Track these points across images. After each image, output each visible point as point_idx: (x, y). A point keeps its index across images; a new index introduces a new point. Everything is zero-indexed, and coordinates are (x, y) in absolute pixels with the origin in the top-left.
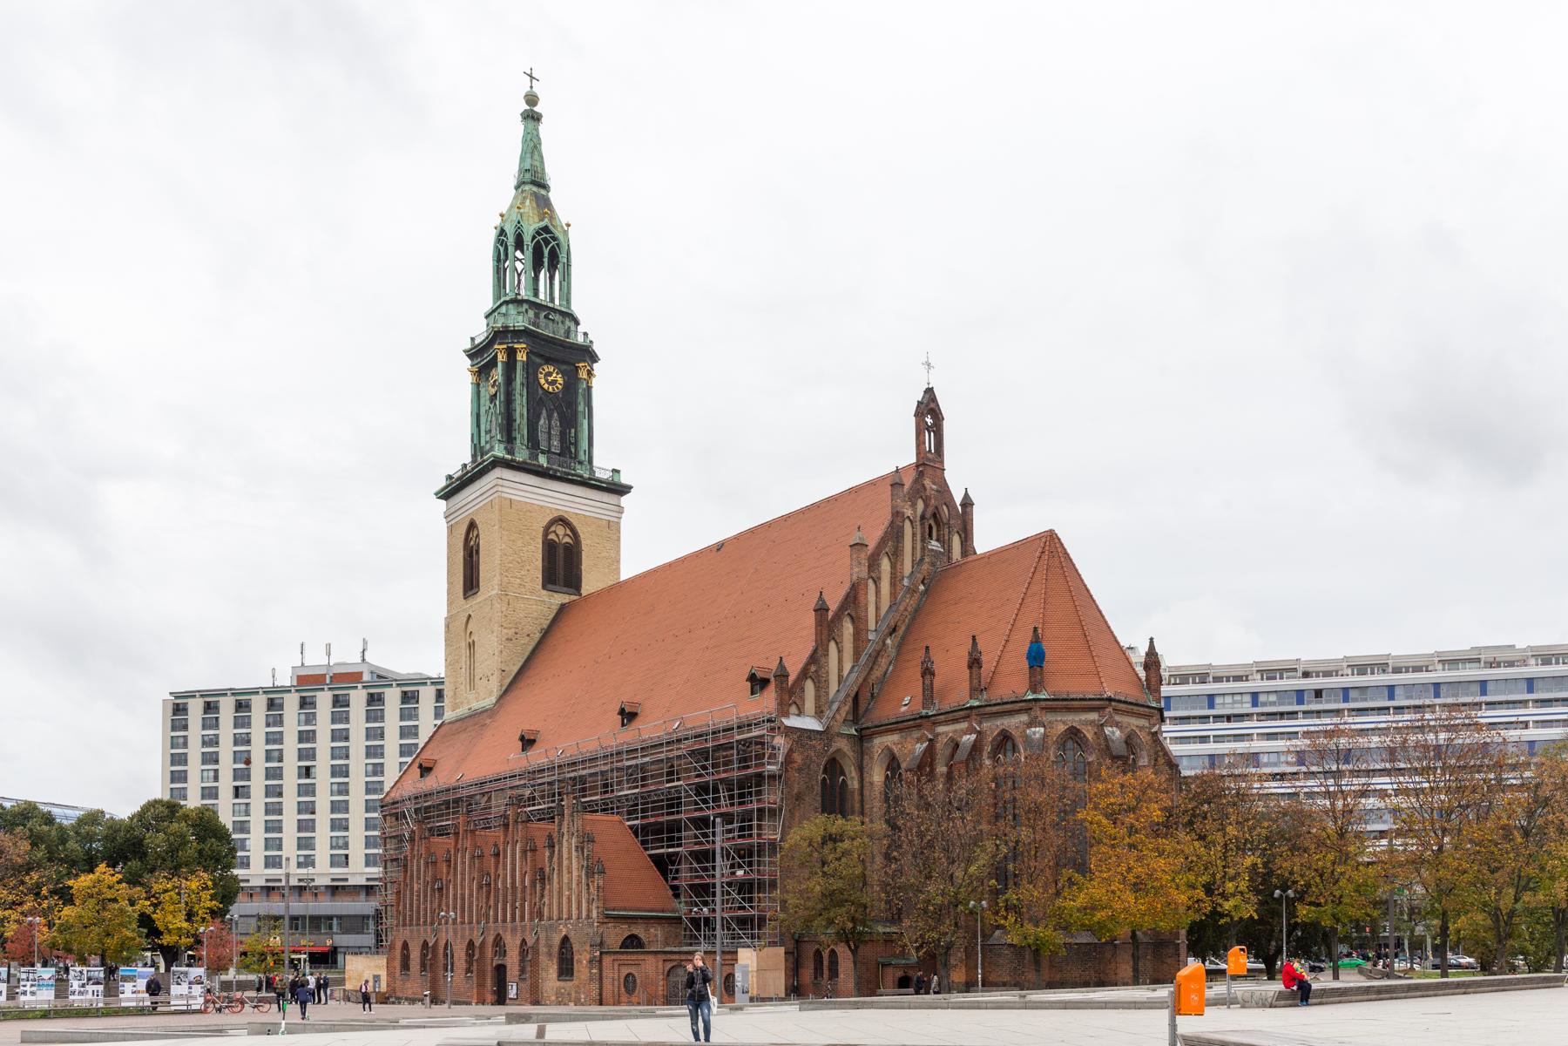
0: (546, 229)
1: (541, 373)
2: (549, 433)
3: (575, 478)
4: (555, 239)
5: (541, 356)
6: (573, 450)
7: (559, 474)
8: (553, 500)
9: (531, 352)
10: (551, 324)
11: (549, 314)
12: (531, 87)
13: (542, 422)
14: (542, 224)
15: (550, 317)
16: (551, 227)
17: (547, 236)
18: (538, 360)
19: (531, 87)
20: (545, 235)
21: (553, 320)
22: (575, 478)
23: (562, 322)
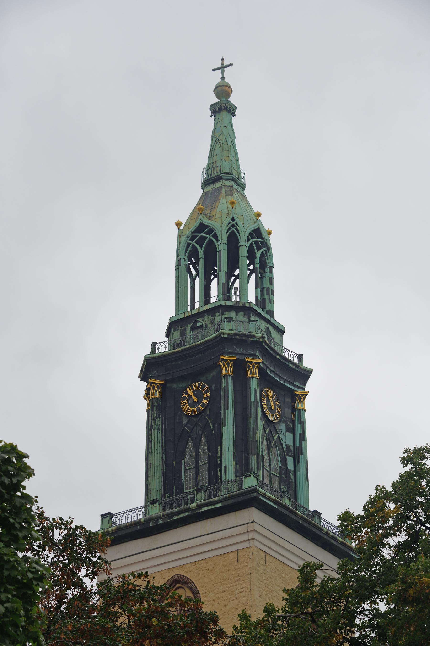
0: (202, 227)
1: (184, 398)
2: (197, 467)
3: (182, 515)
4: (211, 231)
5: (182, 379)
6: (219, 474)
7: (161, 522)
8: (163, 560)
9: (166, 382)
10: (200, 330)
11: (197, 322)
12: (223, 78)
13: (187, 457)
14: (197, 224)
15: (198, 325)
16: (206, 221)
18: (182, 385)
19: (223, 78)
20: (200, 235)
21: (201, 327)
22: (182, 515)
23: (212, 322)
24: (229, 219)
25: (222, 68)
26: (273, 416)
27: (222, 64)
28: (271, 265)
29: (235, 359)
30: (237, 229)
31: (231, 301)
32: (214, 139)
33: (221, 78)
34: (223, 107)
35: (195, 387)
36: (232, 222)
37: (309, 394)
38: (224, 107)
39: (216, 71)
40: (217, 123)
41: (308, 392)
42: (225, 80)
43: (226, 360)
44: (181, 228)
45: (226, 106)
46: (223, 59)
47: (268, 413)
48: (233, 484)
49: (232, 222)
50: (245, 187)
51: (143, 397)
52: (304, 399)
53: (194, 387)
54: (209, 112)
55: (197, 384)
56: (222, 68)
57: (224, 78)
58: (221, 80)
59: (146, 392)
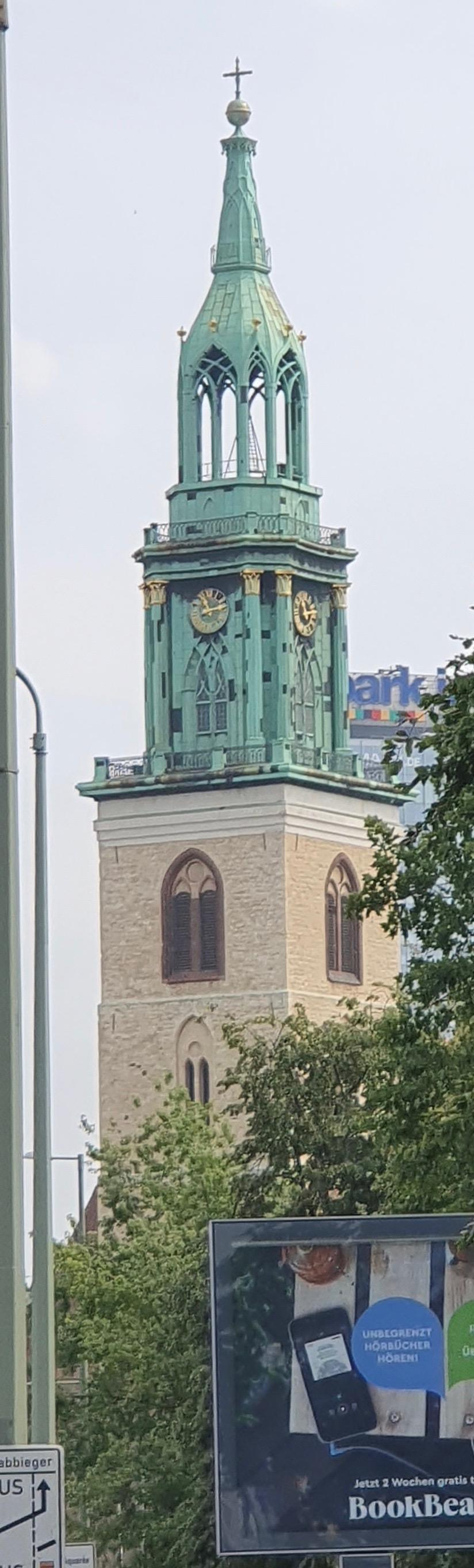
0: (215, 353)
4: (226, 362)
12: (238, 93)
19: (238, 93)
25: (237, 74)
30: (261, 362)
36: (257, 353)
44: (185, 338)
46: (237, 61)
47: (301, 627)
49: (257, 353)
52: (345, 592)
56: (237, 74)
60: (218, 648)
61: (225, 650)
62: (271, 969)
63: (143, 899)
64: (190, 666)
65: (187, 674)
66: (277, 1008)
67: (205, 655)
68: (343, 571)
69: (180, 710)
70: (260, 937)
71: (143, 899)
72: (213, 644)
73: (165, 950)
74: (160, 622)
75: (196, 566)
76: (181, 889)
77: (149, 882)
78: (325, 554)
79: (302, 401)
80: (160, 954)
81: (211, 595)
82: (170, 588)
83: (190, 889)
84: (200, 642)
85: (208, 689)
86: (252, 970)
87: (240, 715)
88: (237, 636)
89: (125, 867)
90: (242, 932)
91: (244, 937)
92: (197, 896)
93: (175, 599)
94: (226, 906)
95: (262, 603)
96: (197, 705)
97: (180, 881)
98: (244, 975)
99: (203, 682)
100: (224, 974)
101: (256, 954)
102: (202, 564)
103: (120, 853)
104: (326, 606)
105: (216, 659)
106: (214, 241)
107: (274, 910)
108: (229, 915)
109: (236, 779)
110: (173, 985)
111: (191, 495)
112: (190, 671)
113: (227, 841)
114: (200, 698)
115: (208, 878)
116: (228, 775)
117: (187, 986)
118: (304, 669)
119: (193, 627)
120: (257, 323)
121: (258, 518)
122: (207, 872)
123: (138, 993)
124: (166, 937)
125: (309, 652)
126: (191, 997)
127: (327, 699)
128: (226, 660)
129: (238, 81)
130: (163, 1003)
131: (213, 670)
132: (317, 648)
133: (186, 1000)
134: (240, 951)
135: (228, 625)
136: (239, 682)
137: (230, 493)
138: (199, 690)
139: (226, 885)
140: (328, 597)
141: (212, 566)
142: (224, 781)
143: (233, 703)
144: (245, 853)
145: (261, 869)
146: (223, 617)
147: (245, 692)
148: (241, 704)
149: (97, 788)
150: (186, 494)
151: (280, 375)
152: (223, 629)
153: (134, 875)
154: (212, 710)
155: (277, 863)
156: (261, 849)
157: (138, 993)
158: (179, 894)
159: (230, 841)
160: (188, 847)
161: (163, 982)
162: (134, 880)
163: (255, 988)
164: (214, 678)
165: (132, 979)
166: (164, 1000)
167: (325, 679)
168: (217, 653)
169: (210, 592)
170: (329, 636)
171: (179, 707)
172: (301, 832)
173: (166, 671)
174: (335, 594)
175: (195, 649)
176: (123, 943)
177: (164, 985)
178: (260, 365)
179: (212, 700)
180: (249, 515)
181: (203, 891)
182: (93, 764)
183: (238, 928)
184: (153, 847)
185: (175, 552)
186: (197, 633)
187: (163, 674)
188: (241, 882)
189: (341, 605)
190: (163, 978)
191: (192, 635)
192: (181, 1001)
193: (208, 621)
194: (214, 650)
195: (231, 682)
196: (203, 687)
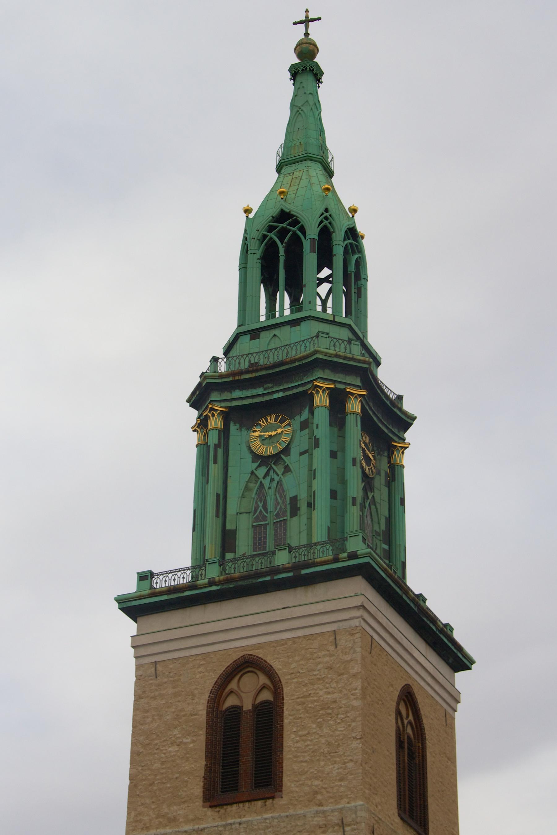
4: (296, 222)
12: (307, 34)
17: (284, 225)
19: (307, 34)
20: (281, 225)
24: (322, 210)
25: (307, 21)
26: (369, 469)
27: (307, 17)
28: (365, 277)
29: (332, 386)
30: (330, 223)
31: (326, 313)
32: (295, 110)
33: (305, 34)
34: (308, 69)
35: (270, 419)
36: (325, 214)
37: (410, 446)
38: (309, 68)
39: (297, 25)
40: (299, 88)
41: (409, 444)
42: (310, 37)
43: (320, 387)
44: (251, 216)
45: (311, 69)
46: (307, 11)
48: (322, 547)
49: (325, 214)
50: (333, 175)
51: (192, 428)
52: (403, 453)
53: (269, 420)
54: (289, 75)
55: (273, 417)
56: (307, 21)
57: (309, 34)
58: (304, 37)
59: (199, 422)
60: (279, 469)
61: (287, 469)
62: (341, 780)
63: (184, 716)
64: (247, 488)
65: (243, 496)
66: (349, 825)
67: (264, 478)
68: (401, 433)
69: (234, 532)
70: (329, 744)
71: (184, 716)
72: (273, 466)
73: (208, 769)
74: (216, 446)
75: (260, 391)
76: (231, 701)
77: (194, 695)
78: (388, 403)
79: (363, 280)
80: (202, 773)
81: (273, 420)
82: (227, 416)
83: (241, 701)
84: (259, 466)
85: (266, 509)
86: (316, 783)
87: (304, 528)
88: (302, 454)
89: (165, 683)
90: (305, 741)
91: (308, 745)
92: (250, 708)
93: (233, 428)
94: (286, 713)
95: (331, 425)
96: (253, 526)
97: (231, 692)
98: (306, 789)
99: (261, 505)
100: (281, 791)
101: (322, 763)
102: (265, 390)
103: (159, 668)
104: (385, 460)
105: (277, 479)
106: (282, 141)
107: (347, 712)
108: (290, 723)
109: (304, 572)
110: (218, 809)
111: (255, 334)
112: (245, 494)
113: (290, 643)
114: (257, 519)
115: (264, 687)
116: (297, 567)
117: (235, 807)
118: (365, 507)
119: (252, 452)
120: (328, 189)
121: (330, 339)
122: (263, 679)
123: (173, 821)
124: (210, 754)
125: (370, 495)
126: (239, 820)
127: (386, 547)
128: (288, 481)
129: (307, 28)
130: (202, 830)
131: (272, 492)
132: (377, 494)
133: (234, 823)
134: (302, 762)
135: (293, 446)
136: (303, 496)
137: (298, 328)
138: (255, 511)
139: (286, 690)
140: (386, 454)
141: (276, 389)
142: (291, 574)
143: (295, 519)
144: (312, 654)
145: (330, 668)
146: (285, 438)
147: (310, 505)
148: (304, 519)
149: (141, 597)
150: (248, 336)
151: (346, 242)
152: (286, 451)
153: (176, 690)
154: (270, 531)
155: (351, 660)
156: (332, 648)
157: (173, 821)
158: (228, 709)
159: (294, 643)
160: (241, 654)
161: (204, 807)
162: (176, 695)
163: (321, 805)
164: (273, 497)
165: (165, 806)
166: (202, 826)
167: (383, 527)
168: (278, 475)
169: (271, 419)
170: (387, 489)
171: (233, 528)
172: (376, 637)
173: (221, 492)
174: (393, 452)
175: (252, 473)
176: (157, 765)
177: (206, 809)
178: (329, 225)
179: (271, 519)
180: (320, 334)
181: (258, 701)
182: (135, 578)
183: (301, 736)
184: (200, 657)
185: (237, 378)
186: (256, 457)
187: (218, 495)
188: (305, 685)
189: (398, 462)
190: (204, 802)
191: (250, 460)
192: (227, 825)
193: (269, 444)
194: (274, 471)
195: (294, 500)
196: (261, 508)
